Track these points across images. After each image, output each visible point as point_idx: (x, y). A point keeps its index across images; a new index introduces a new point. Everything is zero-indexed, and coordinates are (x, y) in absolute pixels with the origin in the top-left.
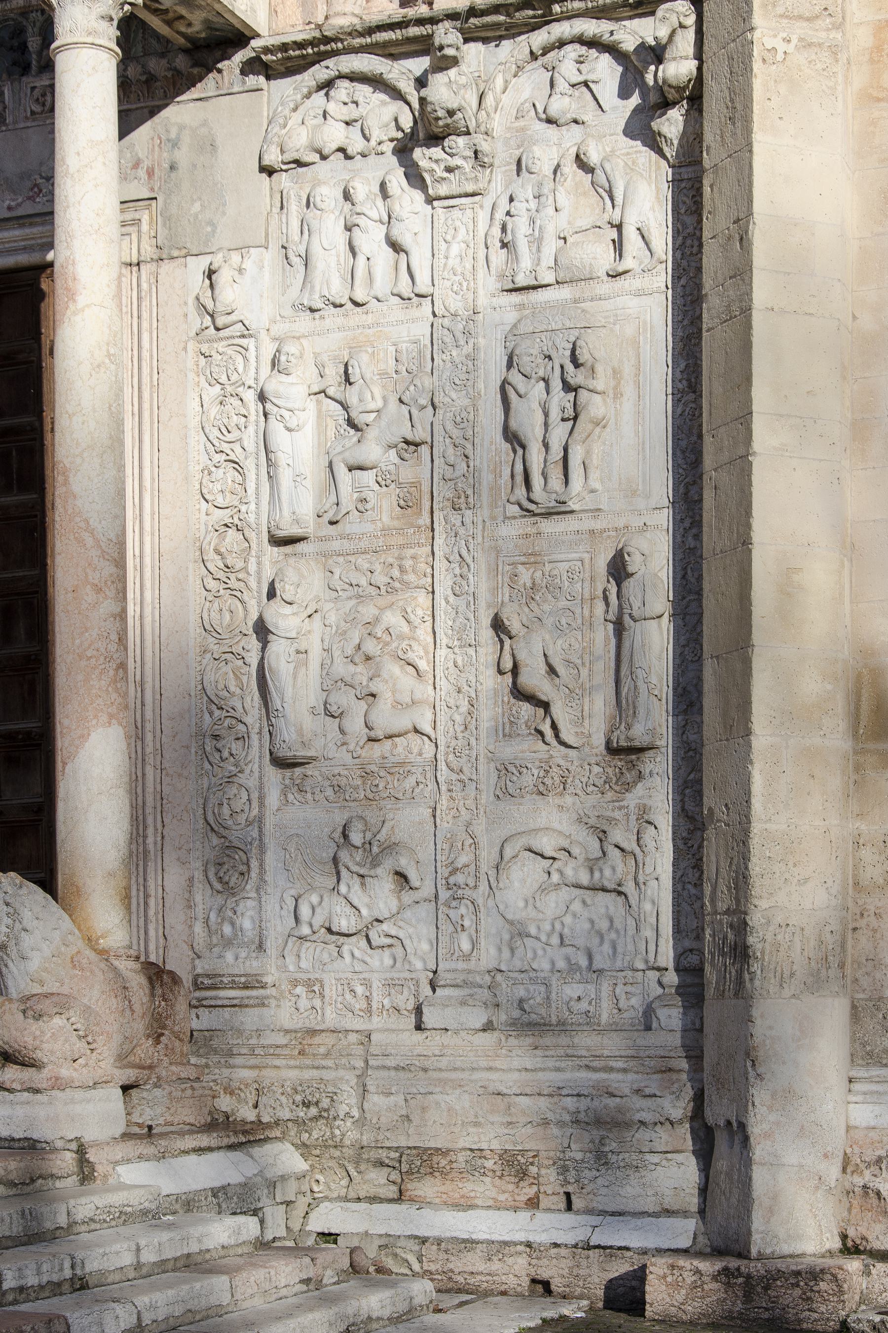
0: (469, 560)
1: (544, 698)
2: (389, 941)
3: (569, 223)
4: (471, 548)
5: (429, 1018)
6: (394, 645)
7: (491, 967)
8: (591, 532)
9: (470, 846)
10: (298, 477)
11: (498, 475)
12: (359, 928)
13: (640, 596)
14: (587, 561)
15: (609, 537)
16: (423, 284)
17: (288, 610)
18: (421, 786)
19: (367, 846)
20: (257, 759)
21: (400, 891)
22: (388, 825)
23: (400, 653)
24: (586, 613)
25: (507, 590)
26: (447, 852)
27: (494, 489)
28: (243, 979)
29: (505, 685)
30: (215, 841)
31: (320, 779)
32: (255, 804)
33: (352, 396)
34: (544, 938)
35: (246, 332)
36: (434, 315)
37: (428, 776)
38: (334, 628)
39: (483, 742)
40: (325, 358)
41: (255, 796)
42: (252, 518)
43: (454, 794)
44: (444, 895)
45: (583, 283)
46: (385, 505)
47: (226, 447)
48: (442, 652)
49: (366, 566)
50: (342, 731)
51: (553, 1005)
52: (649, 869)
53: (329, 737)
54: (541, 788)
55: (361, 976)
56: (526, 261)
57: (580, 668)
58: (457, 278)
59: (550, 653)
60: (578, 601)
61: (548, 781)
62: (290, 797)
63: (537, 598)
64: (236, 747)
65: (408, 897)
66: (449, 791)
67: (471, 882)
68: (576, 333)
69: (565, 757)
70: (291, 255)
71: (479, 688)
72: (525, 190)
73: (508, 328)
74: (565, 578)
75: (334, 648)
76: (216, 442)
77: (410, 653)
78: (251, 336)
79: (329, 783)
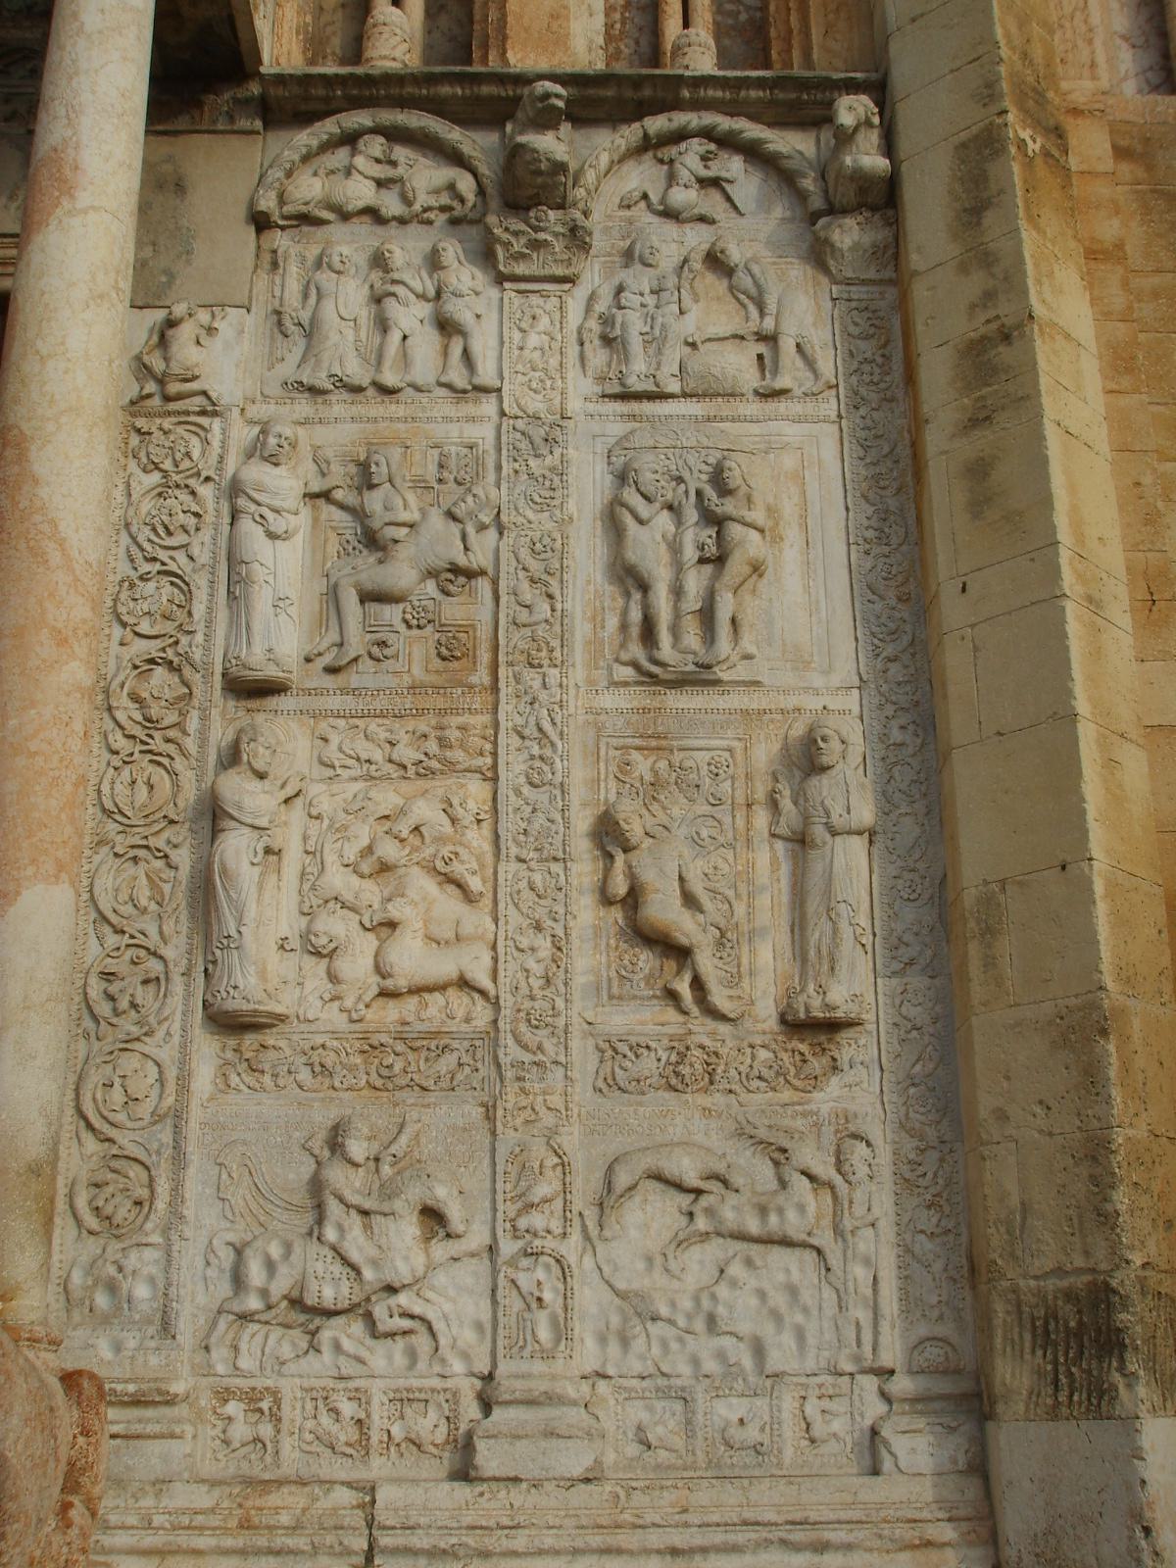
0: (555, 738)
1: (684, 941)
2: (406, 1324)
3: (698, 328)
4: (558, 720)
5: (489, 1458)
6: (428, 851)
7: (588, 1369)
8: (745, 713)
9: (554, 1167)
10: (278, 603)
11: (597, 622)
12: (356, 1299)
13: (842, 801)
14: (739, 753)
15: (772, 721)
16: (487, 374)
17: (255, 785)
18: (467, 1070)
19: (372, 1164)
20: (178, 1016)
21: (428, 1240)
22: (409, 1131)
23: (440, 865)
24: (740, 823)
25: (613, 784)
26: (513, 1176)
27: (595, 645)
28: (131, 1388)
29: (611, 921)
30: (91, 1145)
31: (288, 1052)
32: (171, 1087)
33: (374, 501)
34: (682, 1322)
35: (209, 408)
36: (503, 414)
37: (479, 1055)
38: (326, 822)
39: (577, 1005)
40: (329, 453)
41: (171, 1074)
42: (197, 655)
43: (527, 1085)
44: (508, 1247)
45: (720, 399)
46: (418, 652)
47: (163, 555)
48: (509, 869)
49: (383, 735)
50: (333, 978)
51: (700, 1434)
52: (859, 1210)
53: (309, 985)
54: (673, 1081)
55: (351, 1385)
56: (639, 365)
57: (733, 901)
58: (537, 374)
59: (689, 876)
60: (727, 807)
61: (685, 1070)
62: (234, 1080)
63: (662, 797)
64: (145, 996)
65: (441, 1250)
66: (519, 1079)
67: (556, 1226)
68: (719, 454)
69: (712, 1034)
70: (288, 323)
71: (571, 924)
72: (640, 280)
73: (613, 441)
74: (704, 771)
75: (326, 851)
76: (147, 546)
77: (455, 862)
78: (215, 414)
79: (304, 1059)
